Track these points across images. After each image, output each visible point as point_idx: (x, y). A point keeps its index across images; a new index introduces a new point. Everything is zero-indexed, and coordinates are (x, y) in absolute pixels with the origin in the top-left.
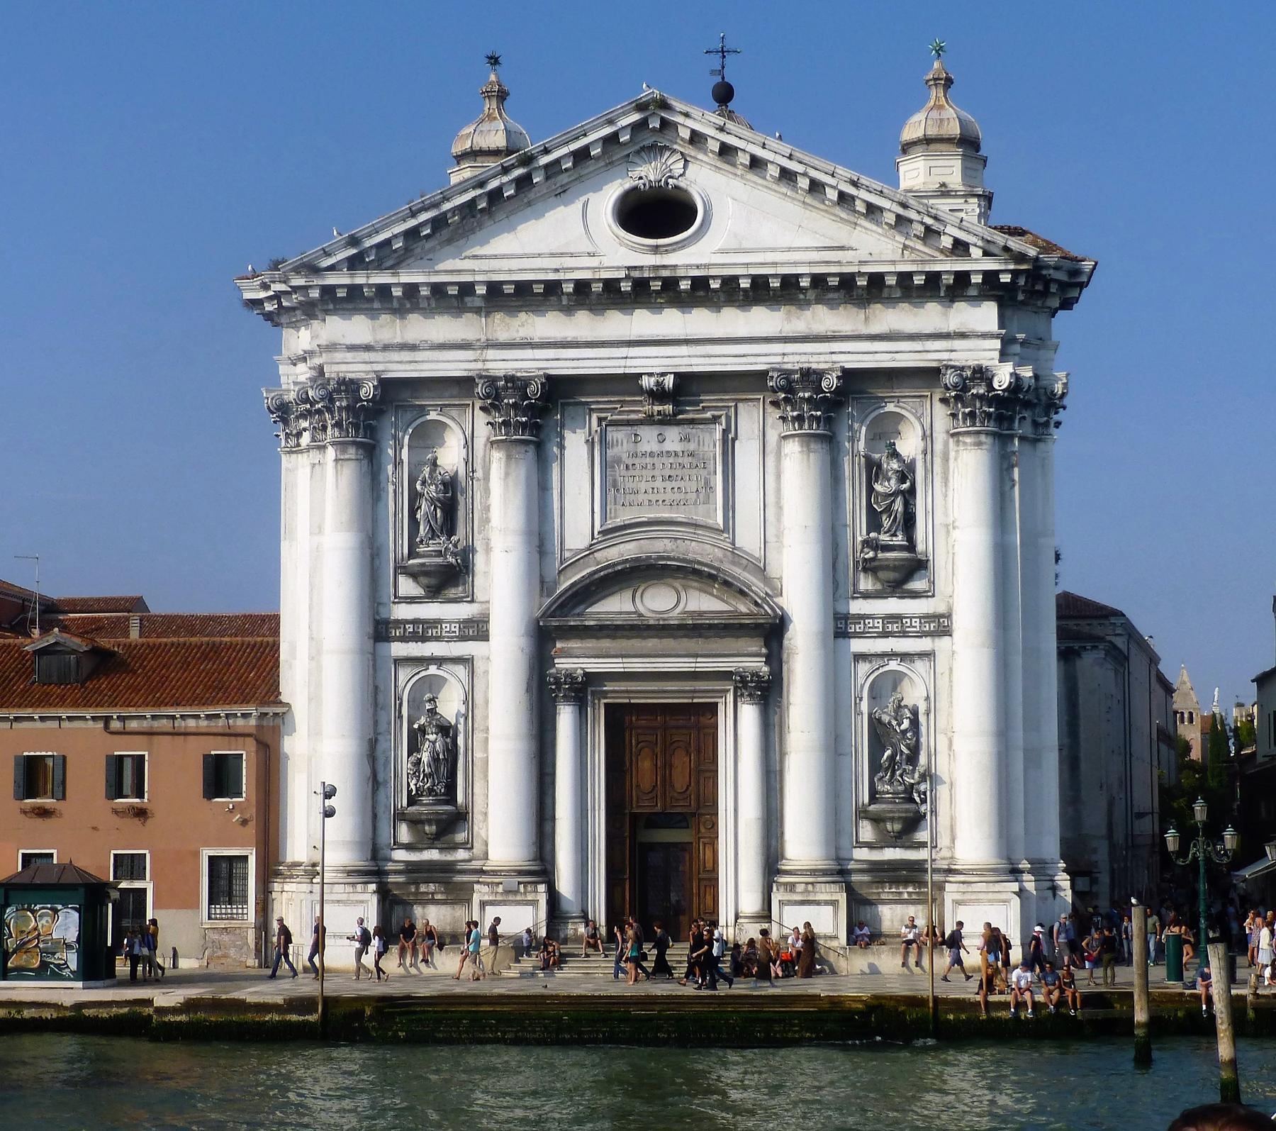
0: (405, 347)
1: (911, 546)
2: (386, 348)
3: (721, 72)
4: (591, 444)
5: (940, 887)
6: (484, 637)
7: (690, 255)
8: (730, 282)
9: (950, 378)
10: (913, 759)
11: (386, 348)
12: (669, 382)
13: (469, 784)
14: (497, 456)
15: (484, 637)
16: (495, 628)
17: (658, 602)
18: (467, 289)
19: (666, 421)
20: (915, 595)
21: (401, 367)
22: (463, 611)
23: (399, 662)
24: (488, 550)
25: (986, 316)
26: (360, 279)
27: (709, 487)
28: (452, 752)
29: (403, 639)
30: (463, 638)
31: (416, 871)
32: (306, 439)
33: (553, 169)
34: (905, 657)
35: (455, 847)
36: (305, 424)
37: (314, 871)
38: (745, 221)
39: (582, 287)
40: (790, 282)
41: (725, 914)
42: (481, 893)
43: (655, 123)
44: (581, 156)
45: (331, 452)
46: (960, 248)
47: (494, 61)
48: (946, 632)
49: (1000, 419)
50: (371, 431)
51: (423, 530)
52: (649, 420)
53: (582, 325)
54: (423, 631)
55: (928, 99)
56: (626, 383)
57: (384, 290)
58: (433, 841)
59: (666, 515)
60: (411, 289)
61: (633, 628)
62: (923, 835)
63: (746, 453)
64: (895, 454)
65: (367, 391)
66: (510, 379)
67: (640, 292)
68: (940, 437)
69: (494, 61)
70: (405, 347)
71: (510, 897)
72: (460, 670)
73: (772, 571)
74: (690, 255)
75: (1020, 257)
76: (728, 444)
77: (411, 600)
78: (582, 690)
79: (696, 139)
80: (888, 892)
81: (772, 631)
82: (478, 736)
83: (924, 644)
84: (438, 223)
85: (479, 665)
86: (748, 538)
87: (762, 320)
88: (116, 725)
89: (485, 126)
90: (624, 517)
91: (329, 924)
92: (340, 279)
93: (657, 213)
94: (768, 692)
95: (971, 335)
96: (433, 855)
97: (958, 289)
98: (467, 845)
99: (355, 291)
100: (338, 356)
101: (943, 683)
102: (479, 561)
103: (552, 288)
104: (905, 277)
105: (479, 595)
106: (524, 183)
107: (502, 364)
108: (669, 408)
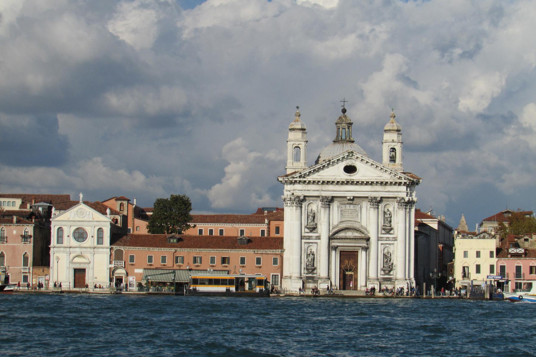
0: (308, 190)
1: (390, 226)
2: (305, 190)
3: (343, 106)
4: (338, 207)
5: (394, 282)
6: (320, 239)
7: (355, 177)
8: (362, 182)
9: (398, 199)
10: (390, 261)
11: (305, 190)
12: (352, 198)
13: (317, 263)
14: (323, 210)
15: (320, 239)
16: (322, 238)
17: (349, 234)
18: (319, 182)
19: (351, 204)
20: (391, 234)
21: (307, 194)
22: (316, 235)
23: (305, 243)
24: (321, 225)
25: (404, 188)
26: (301, 179)
27: (357, 215)
28: (314, 258)
29: (306, 239)
30: (316, 239)
31: (308, 278)
32: (289, 204)
33: (333, 162)
34: (389, 244)
35: (314, 274)
36: (289, 202)
37: (290, 277)
38: (365, 171)
39: (338, 182)
40: (372, 183)
41: (359, 286)
42: (319, 281)
43: (351, 155)
44: (338, 160)
45: (295, 208)
46: (400, 178)
47: (298, 107)
48: (396, 240)
49: (406, 206)
50: (301, 204)
51: (310, 221)
52: (348, 204)
53: (337, 188)
54: (309, 238)
55: (390, 120)
56: (345, 197)
57: (305, 181)
58: (310, 273)
59: (350, 219)
60: (309, 182)
61: (345, 239)
62: (392, 273)
63: (364, 210)
64: (388, 210)
65: (302, 198)
66: (326, 197)
67: (348, 183)
68: (396, 208)
69: (298, 107)
70: (308, 190)
71: (324, 282)
72: (316, 245)
73: (368, 229)
74: (355, 177)
75: (410, 180)
76: (361, 208)
77: (307, 233)
78: (335, 248)
79: (357, 158)
80: (386, 282)
81: (368, 239)
82: (318, 256)
83: (393, 242)
84: (314, 170)
85: (319, 244)
86: (364, 224)
87: (368, 188)
88: (256, 252)
89: (297, 123)
90: (344, 220)
91: (292, 286)
92: (298, 179)
93: (350, 169)
94: (366, 249)
95: (402, 192)
96: (310, 275)
97: (400, 184)
98: (316, 273)
99: (300, 181)
100: (297, 191)
101: (395, 249)
102: (319, 226)
103: (333, 182)
104: (391, 183)
105: (319, 232)
106: (329, 164)
107: (324, 194)
108: (351, 202)
